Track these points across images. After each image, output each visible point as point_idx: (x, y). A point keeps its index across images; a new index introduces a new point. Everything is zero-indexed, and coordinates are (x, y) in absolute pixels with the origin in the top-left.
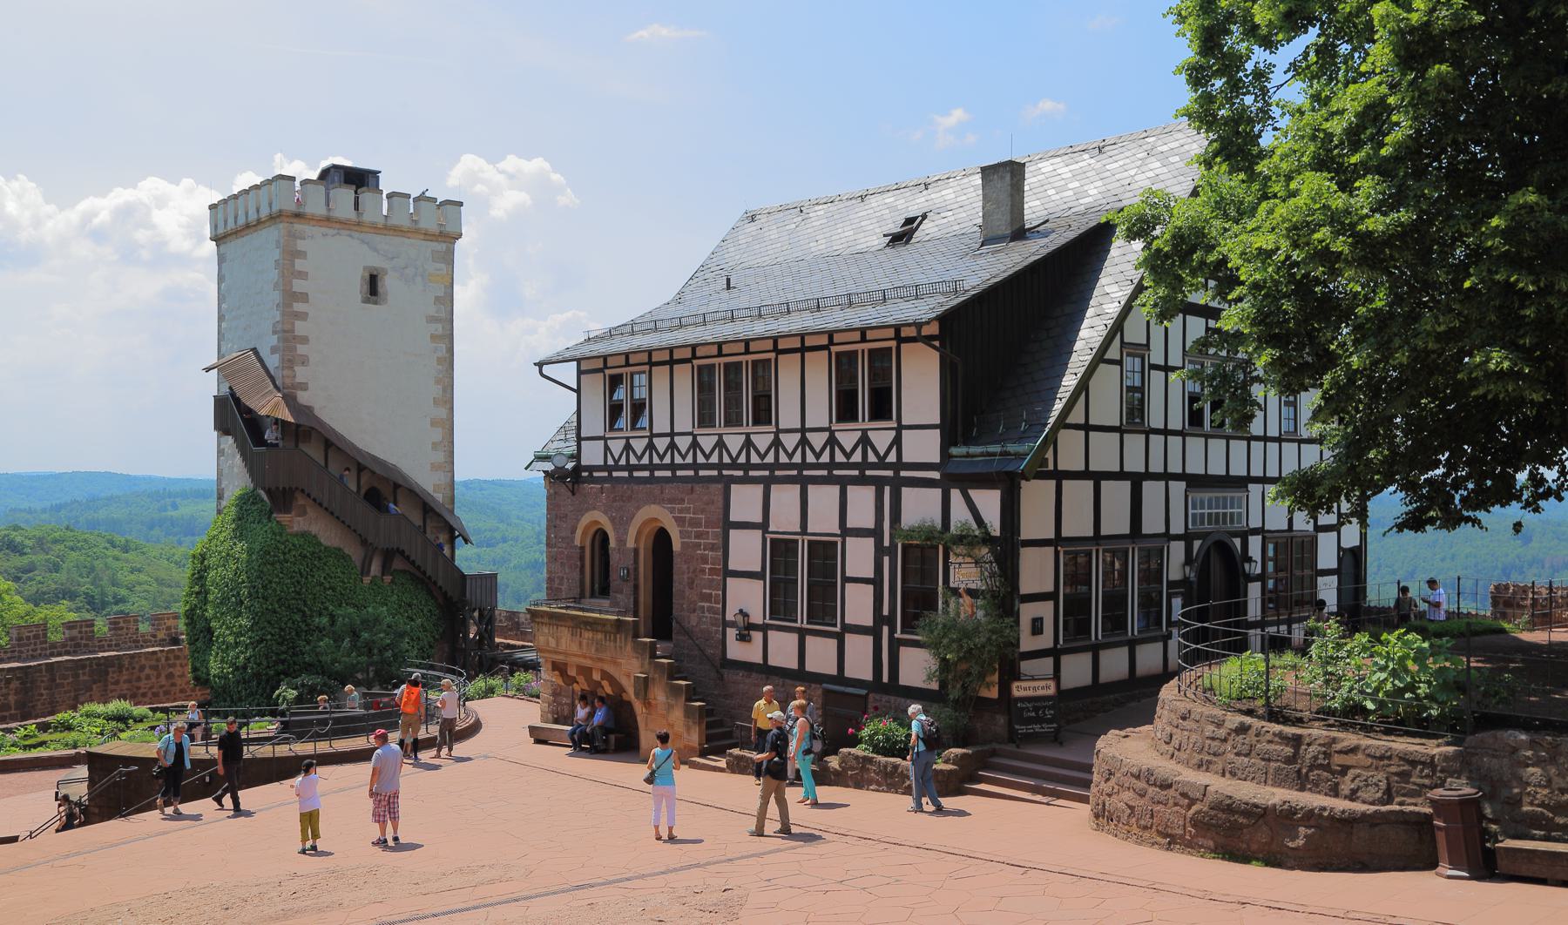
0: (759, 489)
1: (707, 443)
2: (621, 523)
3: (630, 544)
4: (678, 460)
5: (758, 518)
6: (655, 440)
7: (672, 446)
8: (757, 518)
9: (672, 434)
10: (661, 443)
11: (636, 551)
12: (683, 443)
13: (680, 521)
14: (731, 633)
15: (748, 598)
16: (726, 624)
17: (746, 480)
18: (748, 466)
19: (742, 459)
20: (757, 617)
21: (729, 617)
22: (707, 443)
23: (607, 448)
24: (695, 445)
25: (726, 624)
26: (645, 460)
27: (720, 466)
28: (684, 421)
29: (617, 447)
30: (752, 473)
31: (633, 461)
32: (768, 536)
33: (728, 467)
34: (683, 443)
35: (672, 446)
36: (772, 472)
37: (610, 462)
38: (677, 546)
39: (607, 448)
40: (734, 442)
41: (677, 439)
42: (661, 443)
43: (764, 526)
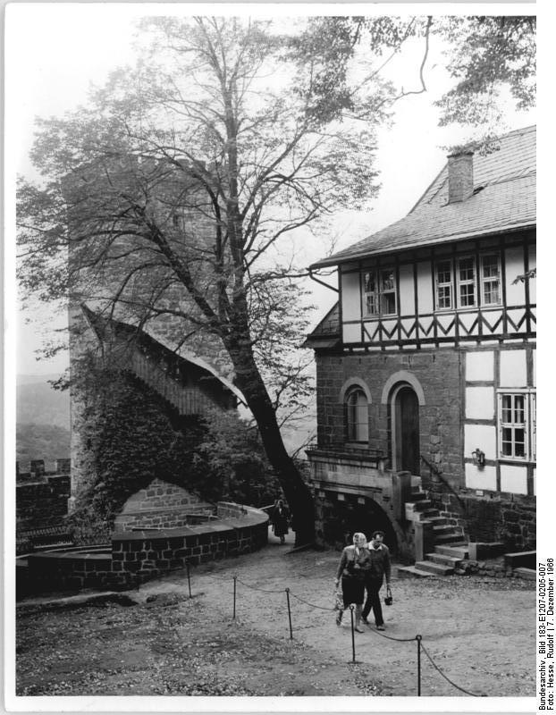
0: (491, 354)
1: (445, 321)
2: (376, 386)
3: (384, 401)
4: (422, 335)
5: (491, 378)
6: (403, 322)
7: (416, 325)
8: (491, 378)
9: (416, 316)
10: (408, 324)
11: (389, 406)
12: (426, 323)
13: (421, 381)
14: (471, 469)
15: (482, 439)
16: (466, 460)
17: (478, 349)
18: (480, 338)
19: (476, 332)
20: (490, 455)
21: (468, 454)
22: (445, 321)
23: (363, 329)
24: (435, 323)
25: (466, 460)
26: (395, 337)
27: (457, 339)
28: (426, 306)
29: (371, 327)
30: (483, 343)
31: (385, 337)
32: (499, 390)
33: (465, 339)
34: (426, 323)
35: (416, 325)
36: (501, 341)
37: (367, 340)
38: (422, 402)
39: (363, 329)
40: (468, 320)
41: (420, 320)
42: (408, 324)
43: (495, 383)
